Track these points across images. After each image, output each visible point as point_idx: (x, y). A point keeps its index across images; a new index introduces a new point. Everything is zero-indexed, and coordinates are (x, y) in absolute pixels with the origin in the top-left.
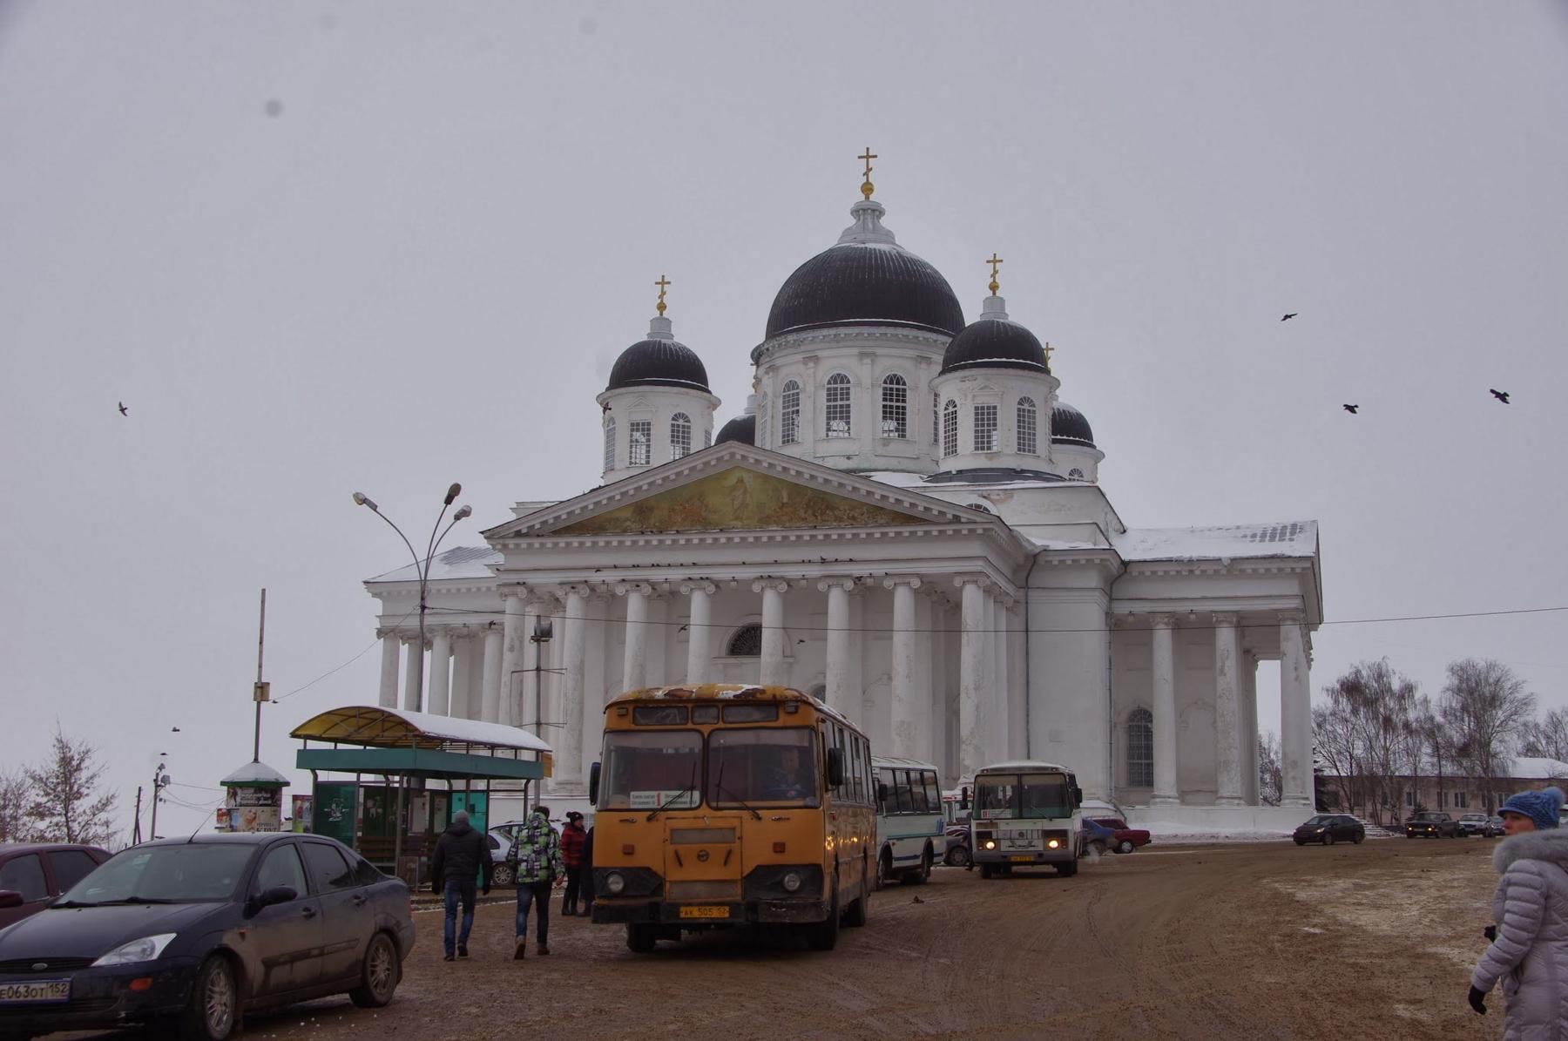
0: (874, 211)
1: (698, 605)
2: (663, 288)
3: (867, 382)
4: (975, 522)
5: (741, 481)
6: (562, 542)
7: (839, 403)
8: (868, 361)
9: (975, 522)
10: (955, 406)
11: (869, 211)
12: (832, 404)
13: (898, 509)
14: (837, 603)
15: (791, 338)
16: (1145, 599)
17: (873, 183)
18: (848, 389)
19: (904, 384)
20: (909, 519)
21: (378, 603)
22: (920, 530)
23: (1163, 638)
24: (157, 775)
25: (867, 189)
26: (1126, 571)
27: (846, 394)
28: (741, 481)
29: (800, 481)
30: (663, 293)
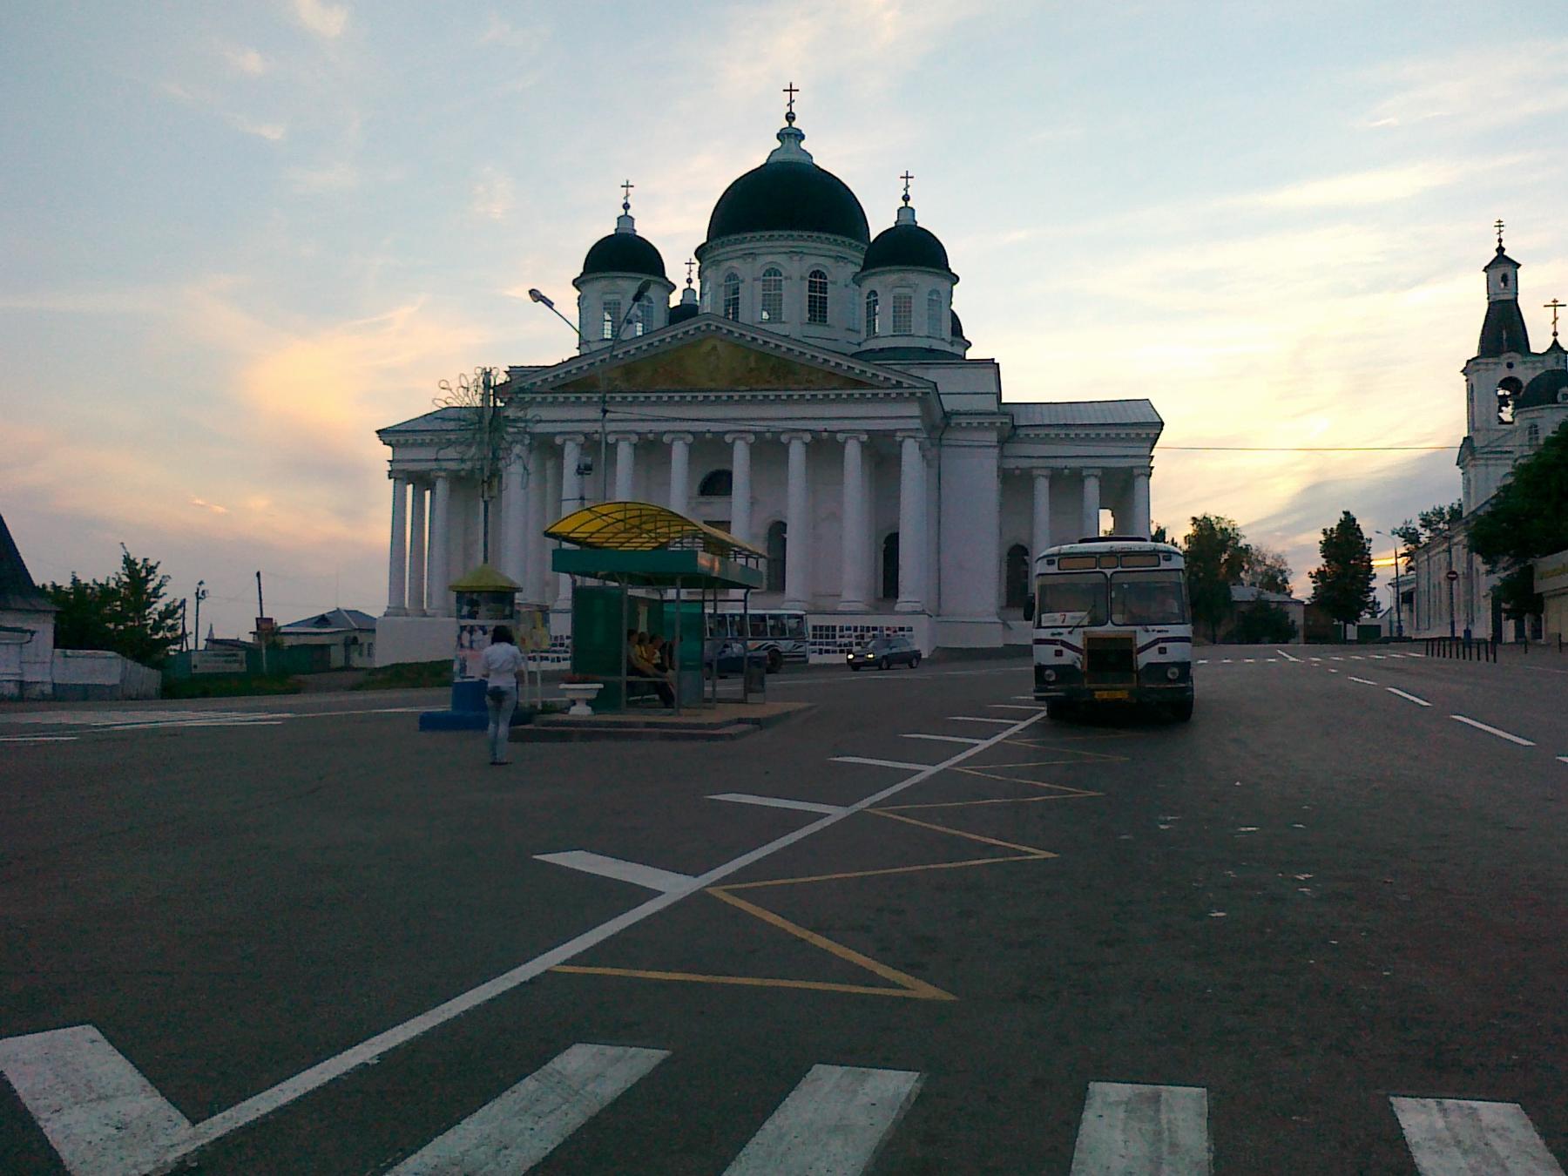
0: (796, 135)
1: (679, 453)
2: (627, 191)
3: (796, 276)
4: (915, 387)
5: (714, 348)
6: (561, 397)
8: (796, 258)
9: (915, 387)
10: (877, 295)
11: (793, 136)
13: (850, 375)
14: (797, 453)
16: (1029, 454)
17: (796, 113)
18: (781, 281)
19: (826, 279)
20: (858, 384)
21: (389, 449)
22: (869, 393)
23: (1042, 486)
24: (198, 590)
25: (790, 117)
26: (1015, 434)
28: (714, 348)
29: (766, 350)
30: (627, 195)
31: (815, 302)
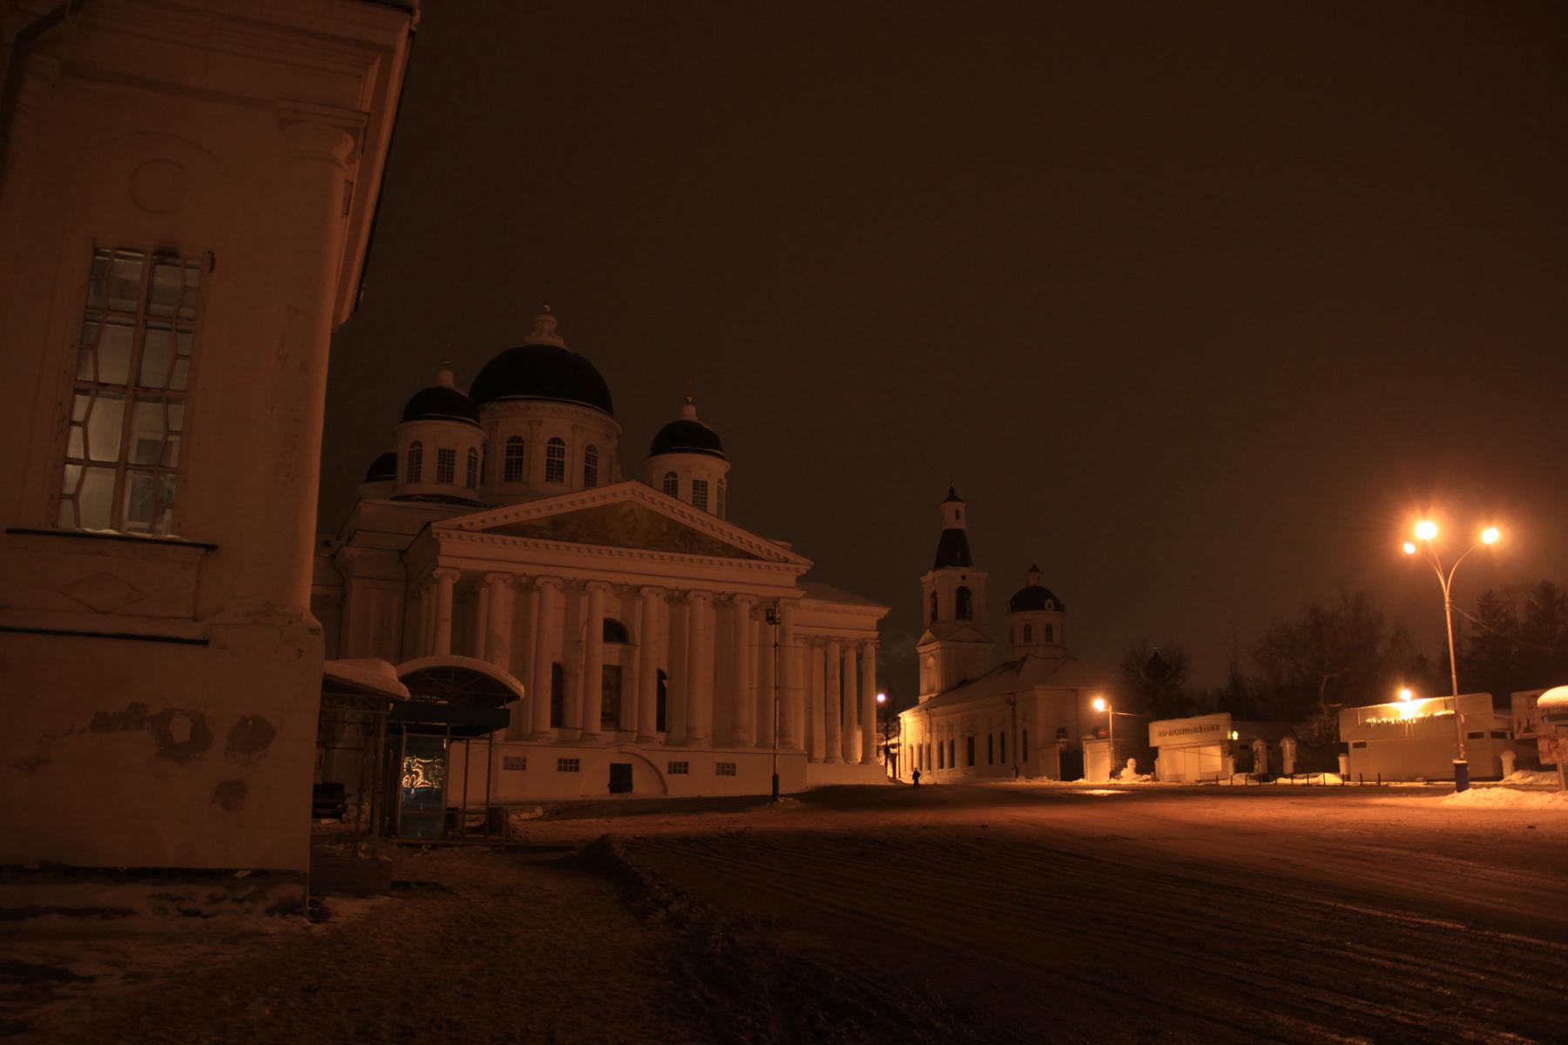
5: (632, 511)
7: (556, 459)
12: (551, 458)
13: (745, 547)
15: (522, 404)
20: (750, 556)
27: (561, 453)
31: (444, 455)
